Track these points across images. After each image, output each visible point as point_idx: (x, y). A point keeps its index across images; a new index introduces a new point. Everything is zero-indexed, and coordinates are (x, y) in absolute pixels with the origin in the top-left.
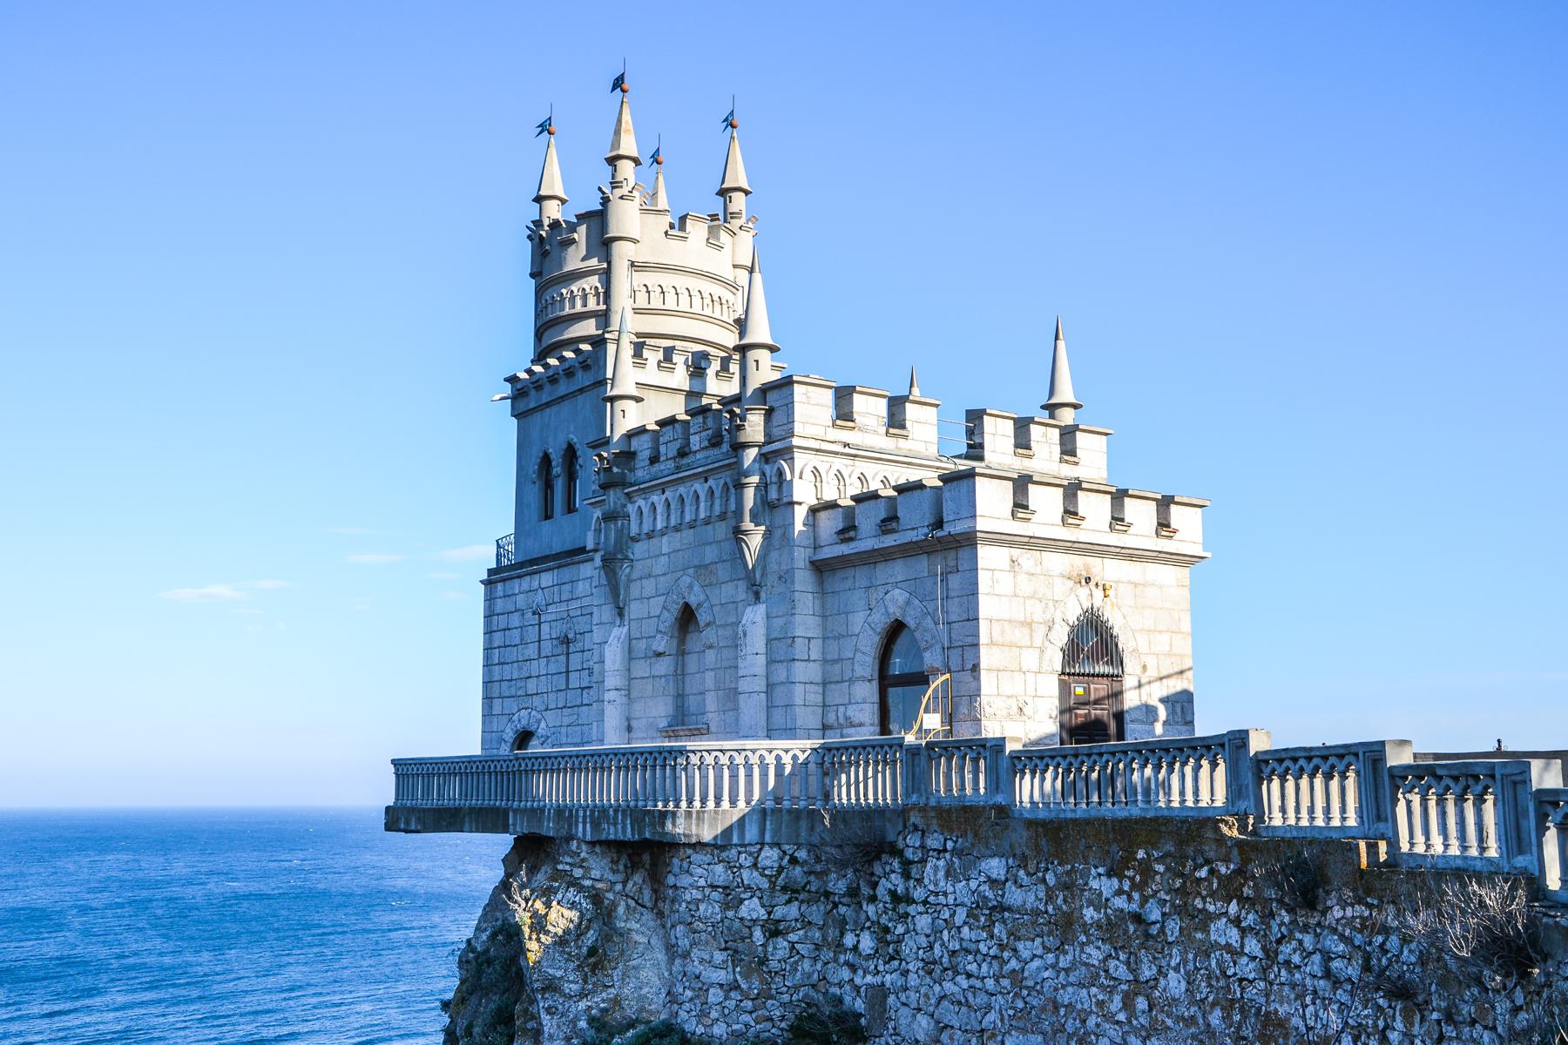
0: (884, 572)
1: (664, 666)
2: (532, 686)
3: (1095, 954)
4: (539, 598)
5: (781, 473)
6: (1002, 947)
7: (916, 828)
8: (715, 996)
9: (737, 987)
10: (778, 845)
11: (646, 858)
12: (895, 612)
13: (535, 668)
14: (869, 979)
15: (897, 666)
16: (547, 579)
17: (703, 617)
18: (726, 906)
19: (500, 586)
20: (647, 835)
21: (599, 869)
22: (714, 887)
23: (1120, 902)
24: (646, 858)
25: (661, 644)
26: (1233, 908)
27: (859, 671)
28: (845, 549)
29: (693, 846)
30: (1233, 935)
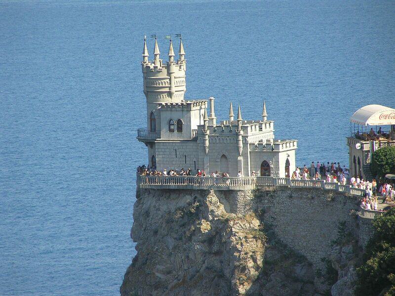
2: (174, 163)
11: (223, 192)
12: (265, 158)
13: (175, 159)
24: (223, 192)
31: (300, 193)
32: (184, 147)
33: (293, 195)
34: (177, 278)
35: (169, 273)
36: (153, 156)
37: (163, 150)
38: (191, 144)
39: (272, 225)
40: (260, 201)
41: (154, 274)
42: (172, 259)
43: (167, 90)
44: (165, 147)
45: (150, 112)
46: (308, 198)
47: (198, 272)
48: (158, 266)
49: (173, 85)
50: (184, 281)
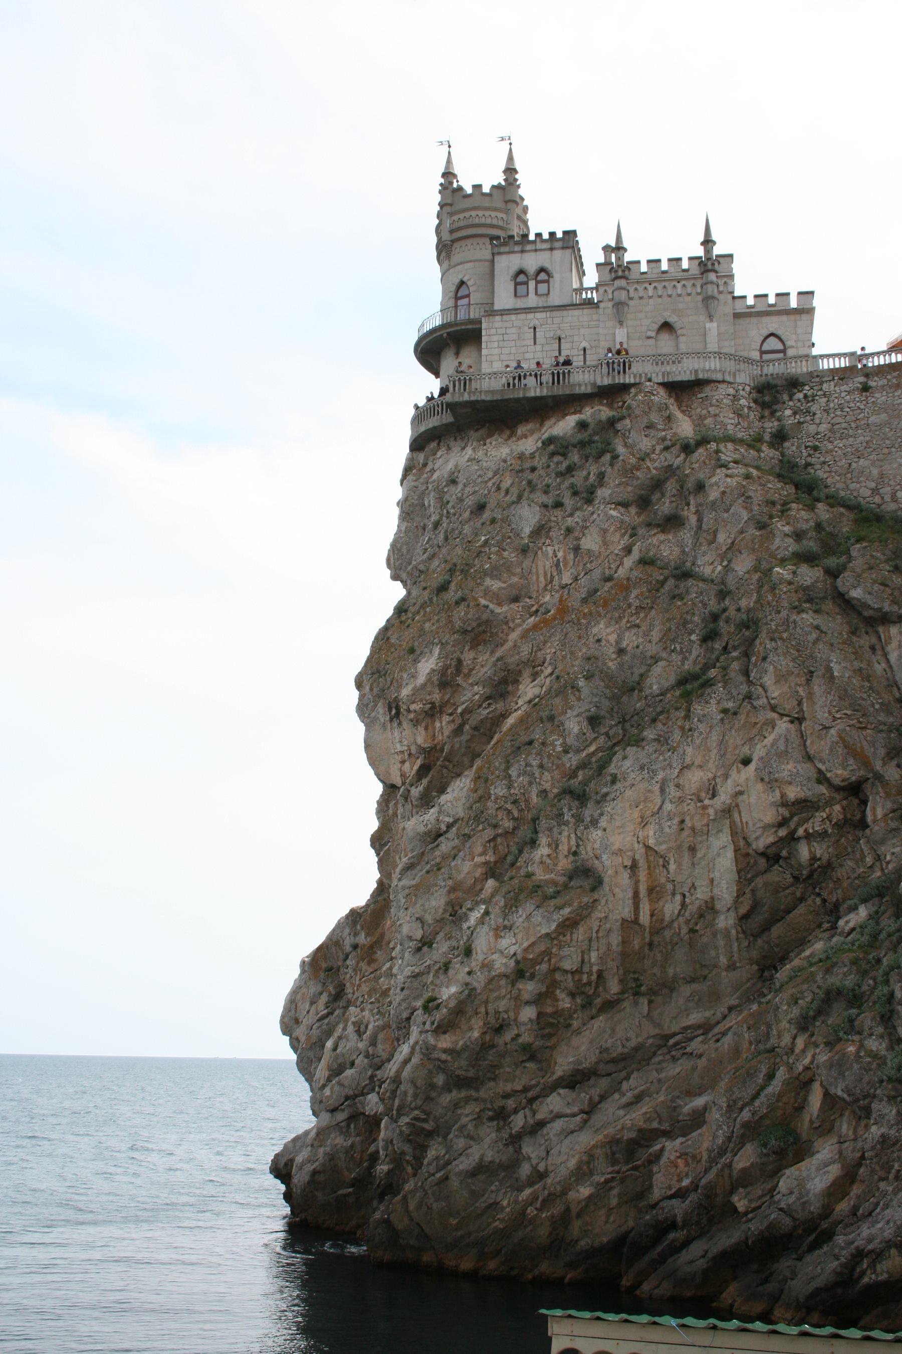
0: (765, 319)
1: (652, 342)
7: (818, 376)
9: (739, 423)
12: (772, 330)
13: (532, 348)
15: (766, 347)
16: (538, 315)
17: (677, 326)
18: (733, 401)
19: (498, 318)
20: (701, 376)
21: (662, 392)
25: (653, 334)
27: (754, 347)
28: (753, 310)
29: (719, 382)
31: (895, 374)
32: (556, 321)
33: (872, 384)
34: (537, 611)
35: (516, 599)
37: (503, 331)
38: (576, 312)
39: (808, 465)
40: (772, 414)
41: (476, 600)
42: (527, 563)
45: (457, 281)
47: (609, 579)
48: (488, 581)
50: (563, 609)
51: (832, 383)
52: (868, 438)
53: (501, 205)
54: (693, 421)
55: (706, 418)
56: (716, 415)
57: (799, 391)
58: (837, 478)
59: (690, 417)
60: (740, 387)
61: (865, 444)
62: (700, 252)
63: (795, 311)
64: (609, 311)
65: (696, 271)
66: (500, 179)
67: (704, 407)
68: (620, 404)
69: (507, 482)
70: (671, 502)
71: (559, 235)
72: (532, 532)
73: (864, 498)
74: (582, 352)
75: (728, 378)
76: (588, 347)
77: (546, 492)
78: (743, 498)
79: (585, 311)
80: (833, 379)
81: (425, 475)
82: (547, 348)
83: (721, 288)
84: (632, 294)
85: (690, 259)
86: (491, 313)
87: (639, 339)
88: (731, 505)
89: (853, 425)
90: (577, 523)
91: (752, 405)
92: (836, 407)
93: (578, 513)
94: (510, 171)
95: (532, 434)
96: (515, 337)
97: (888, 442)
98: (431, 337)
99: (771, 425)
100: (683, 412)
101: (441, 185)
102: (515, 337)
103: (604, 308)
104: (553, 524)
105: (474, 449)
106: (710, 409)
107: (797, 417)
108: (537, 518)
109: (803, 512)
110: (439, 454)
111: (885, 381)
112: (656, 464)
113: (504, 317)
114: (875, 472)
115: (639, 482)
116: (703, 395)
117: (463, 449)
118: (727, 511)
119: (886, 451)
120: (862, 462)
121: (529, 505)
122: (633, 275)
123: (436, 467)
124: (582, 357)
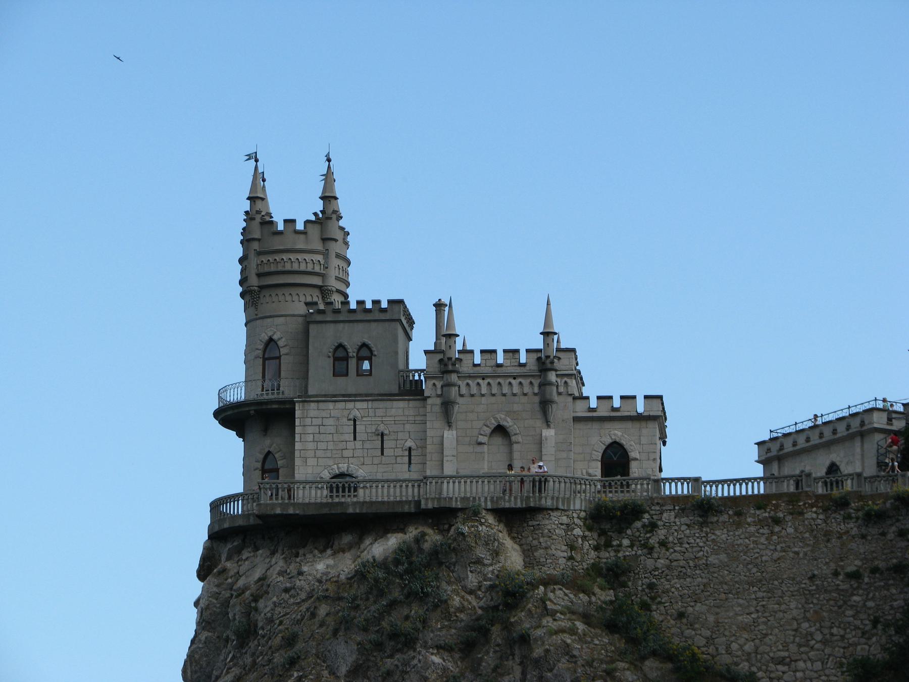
0: (607, 425)
2: (346, 453)
3: (752, 529)
4: (357, 414)
5: (566, 382)
6: (707, 534)
7: (658, 504)
8: (562, 561)
10: (585, 511)
13: (351, 445)
14: (627, 553)
16: (359, 405)
18: (566, 531)
19: (312, 405)
20: (532, 505)
21: (491, 519)
22: (562, 524)
23: (767, 515)
26: (814, 509)
28: (595, 414)
29: (552, 510)
30: (814, 516)
32: (380, 412)
36: (269, 453)
37: (319, 422)
38: (401, 404)
43: (317, 281)
44: (324, 414)
45: (267, 338)
46: (761, 523)
49: (333, 273)
51: (673, 513)
52: (705, 581)
53: (318, 246)
54: (523, 551)
55: (536, 550)
56: (546, 548)
57: (639, 520)
58: (672, 622)
59: (521, 545)
60: (575, 515)
61: (702, 587)
62: (538, 343)
63: (639, 418)
64: (437, 409)
65: (533, 367)
66: (319, 206)
67: (535, 536)
68: (446, 527)
69: (323, 610)
70: (495, 652)
71: (384, 305)
72: (349, 672)
73: (699, 648)
74: (407, 453)
75: (561, 507)
76: (414, 447)
77: (365, 630)
78: (567, 657)
79: (412, 404)
80: (674, 509)
81: (230, 580)
82: (368, 445)
83: (561, 389)
84: (464, 390)
85: (528, 351)
86: (306, 398)
87: (469, 444)
88: (555, 665)
89: (692, 563)
90: (397, 666)
91: (587, 533)
92: (676, 541)
93: (398, 656)
94: (328, 198)
95: (350, 548)
96: (332, 430)
97: (725, 587)
98: (236, 411)
99: (607, 555)
100: (513, 538)
101: (247, 213)
102: (333, 431)
103: (432, 405)
104: (371, 664)
105: (285, 558)
106: (541, 540)
107: (635, 548)
108: (354, 656)
109: (628, 673)
110: (245, 554)
111: (726, 516)
112: (482, 603)
113: (322, 405)
114: (711, 619)
115: (463, 624)
116: (535, 523)
117: (273, 553)
118: (551, 670)
119: (723, 596)
120: (698, 607)
121: (346, 642)
122: (465, 368)
123: (242, 569)
124: (407, 459)
